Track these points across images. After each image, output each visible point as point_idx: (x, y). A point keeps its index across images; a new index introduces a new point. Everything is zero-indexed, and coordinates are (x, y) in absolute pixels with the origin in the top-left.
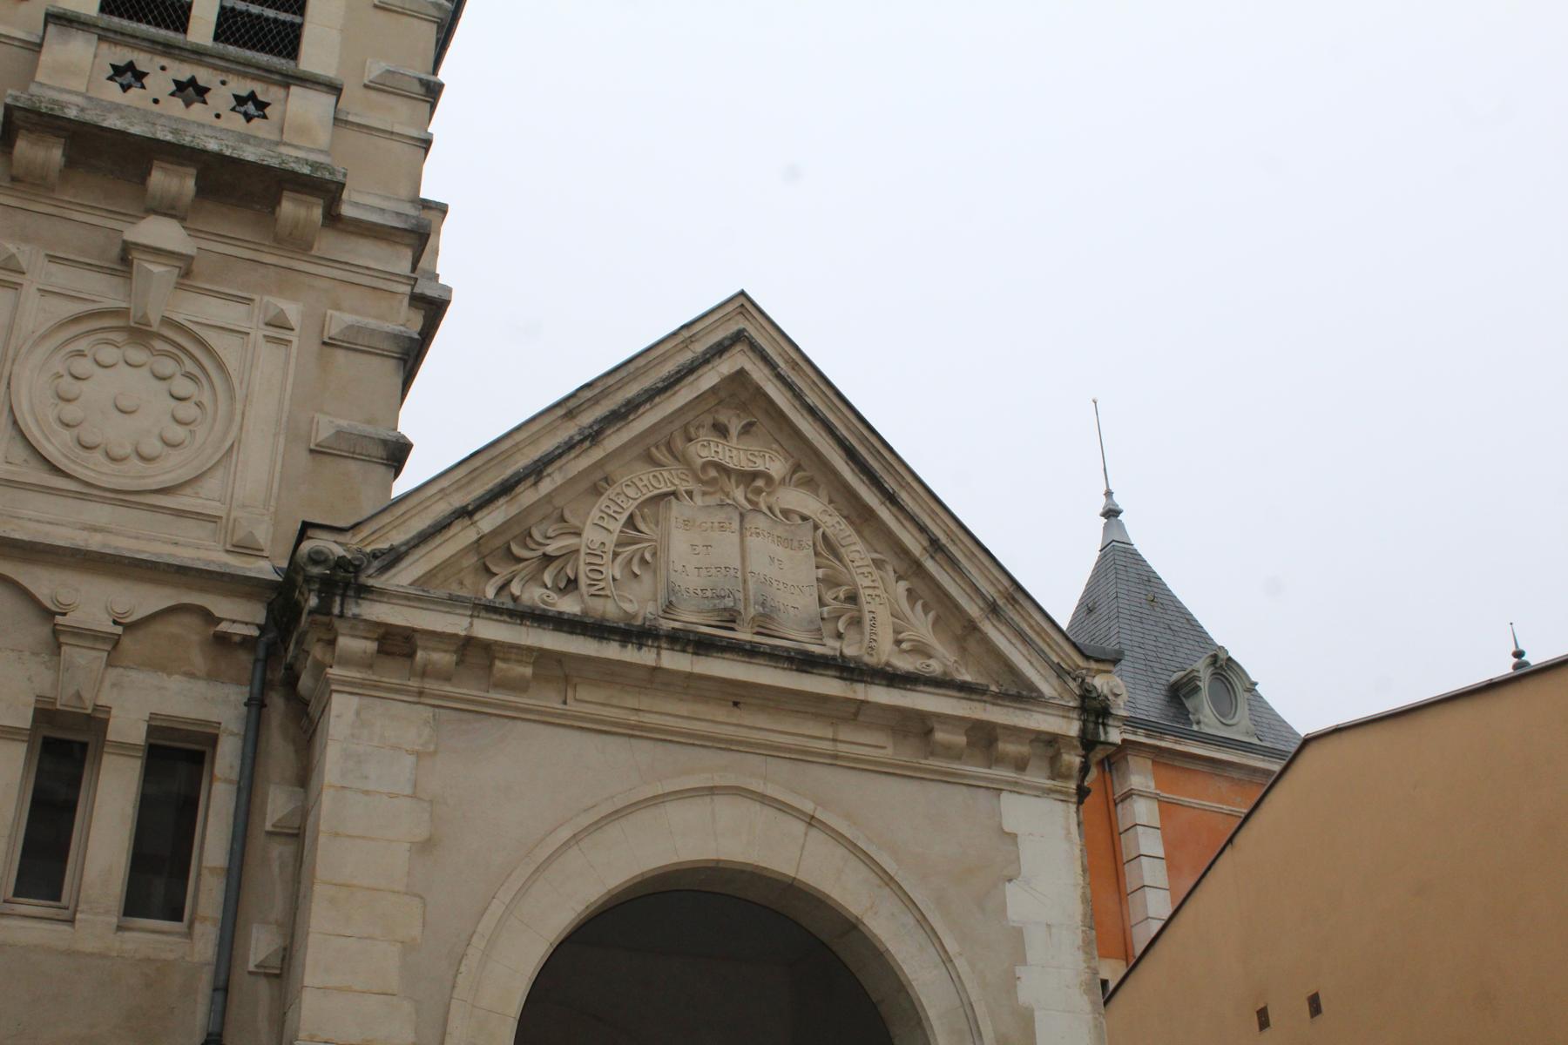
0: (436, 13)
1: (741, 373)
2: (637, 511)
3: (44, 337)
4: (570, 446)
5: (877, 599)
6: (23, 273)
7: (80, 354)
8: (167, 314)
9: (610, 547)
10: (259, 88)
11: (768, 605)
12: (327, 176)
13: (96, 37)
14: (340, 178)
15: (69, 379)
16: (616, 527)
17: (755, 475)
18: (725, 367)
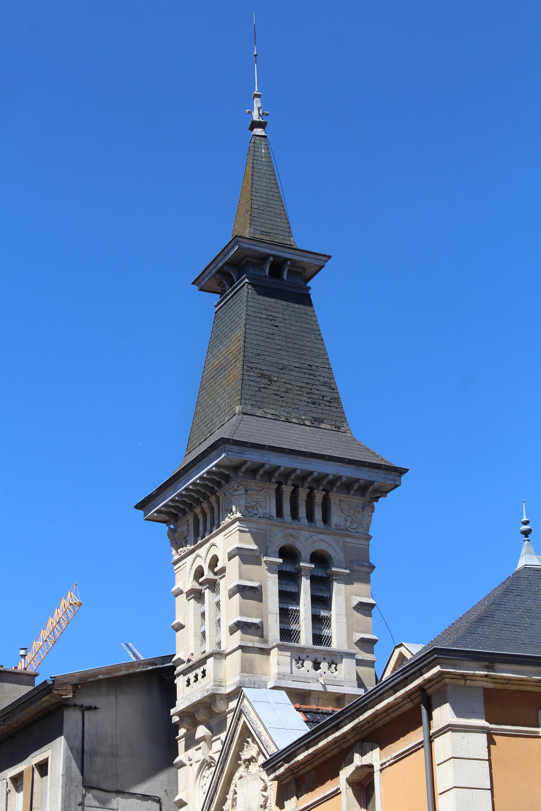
0: (236, 589)
1: (244, 722)
2: (235, 788)
3: (197, 778)
4: (219, 778)
5: (272, 789)
6: (192, 760)
7: (204, 776)
8: (209, 755)
9: (230, 807)
10: (205, 667)
11: (249, 809)
12: (209, 693)
13: (182, 675)
14: (211, 692)
15: (204, 786)
16: (231, 798)
17: (253, 757)
18: (241, 723)
